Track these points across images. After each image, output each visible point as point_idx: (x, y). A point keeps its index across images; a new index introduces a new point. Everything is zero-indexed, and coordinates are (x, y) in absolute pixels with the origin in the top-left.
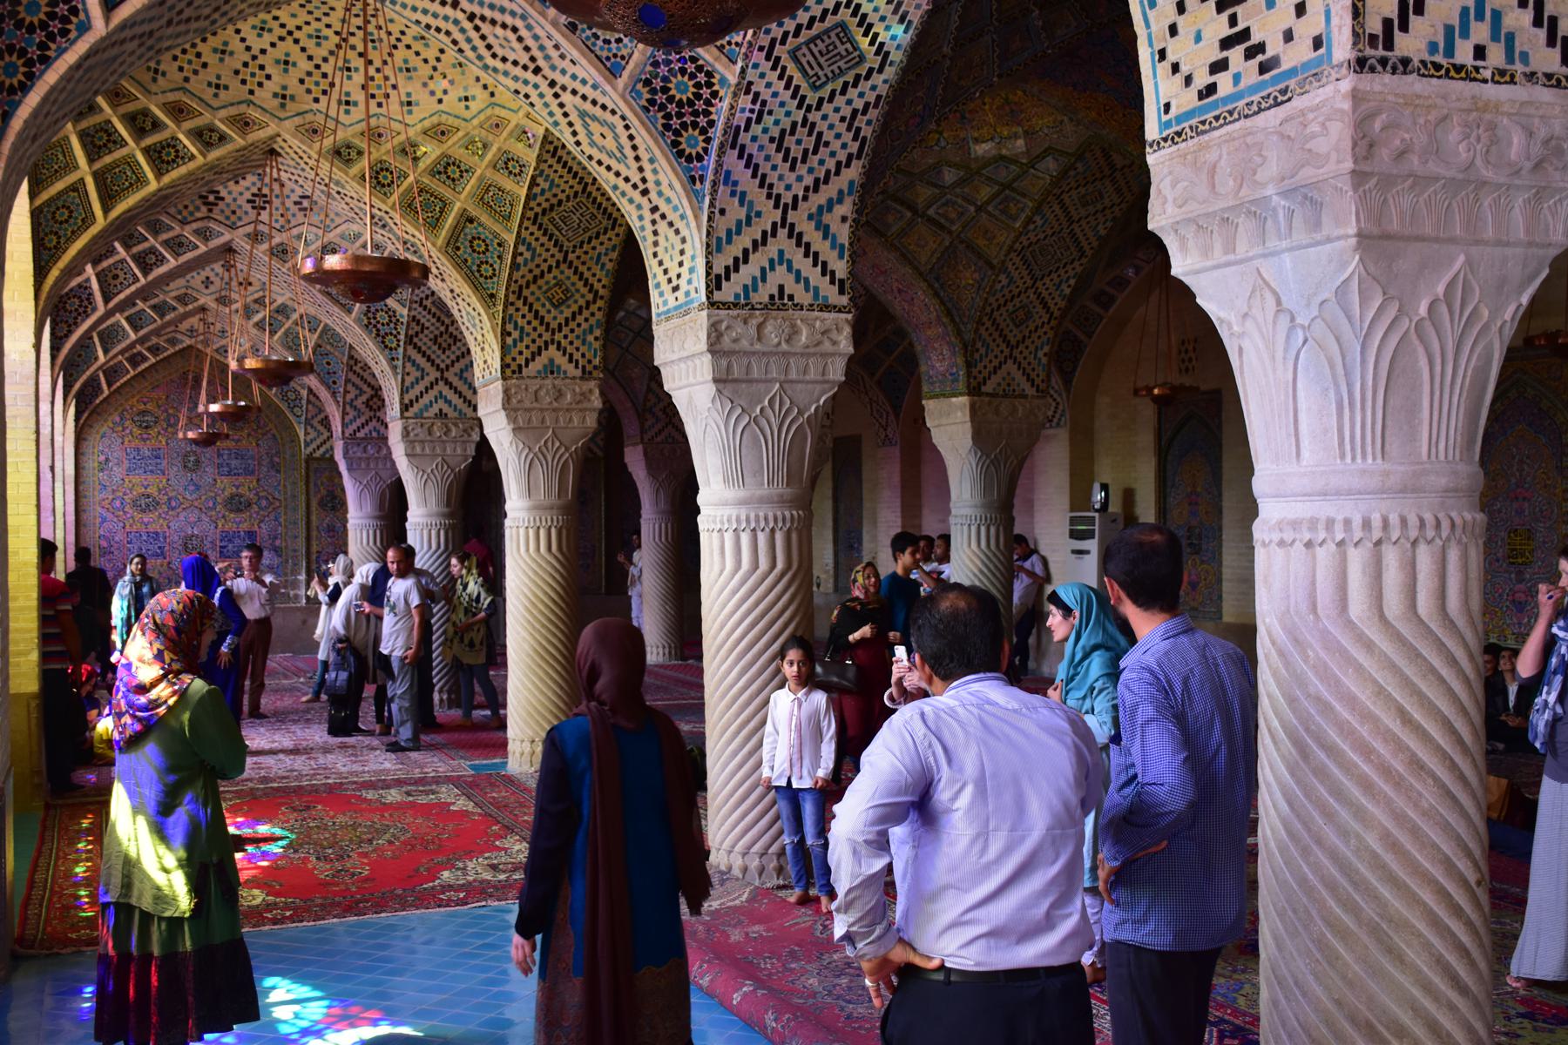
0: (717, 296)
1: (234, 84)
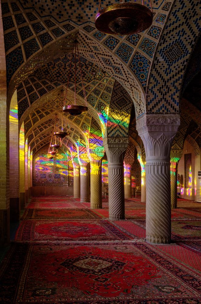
0: (108, 136)
1: (50, 105)
